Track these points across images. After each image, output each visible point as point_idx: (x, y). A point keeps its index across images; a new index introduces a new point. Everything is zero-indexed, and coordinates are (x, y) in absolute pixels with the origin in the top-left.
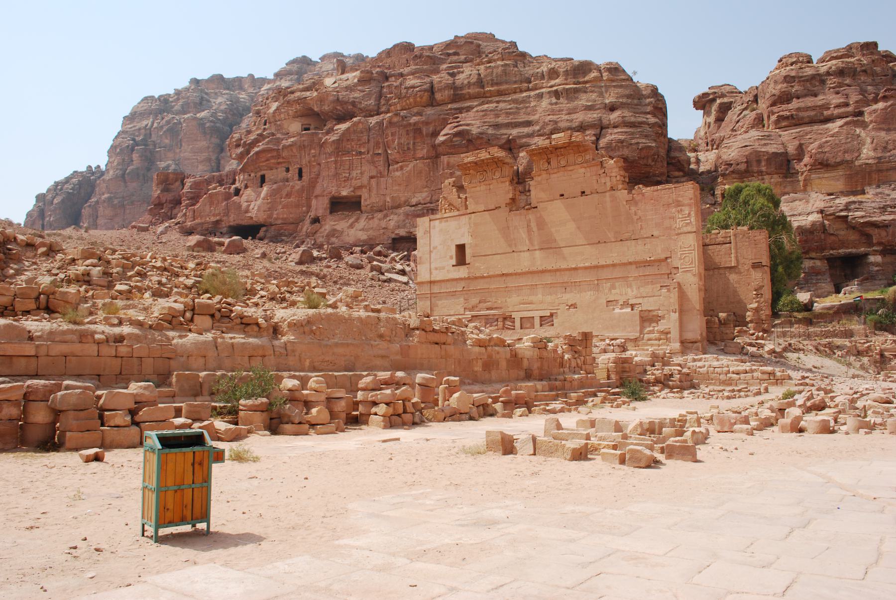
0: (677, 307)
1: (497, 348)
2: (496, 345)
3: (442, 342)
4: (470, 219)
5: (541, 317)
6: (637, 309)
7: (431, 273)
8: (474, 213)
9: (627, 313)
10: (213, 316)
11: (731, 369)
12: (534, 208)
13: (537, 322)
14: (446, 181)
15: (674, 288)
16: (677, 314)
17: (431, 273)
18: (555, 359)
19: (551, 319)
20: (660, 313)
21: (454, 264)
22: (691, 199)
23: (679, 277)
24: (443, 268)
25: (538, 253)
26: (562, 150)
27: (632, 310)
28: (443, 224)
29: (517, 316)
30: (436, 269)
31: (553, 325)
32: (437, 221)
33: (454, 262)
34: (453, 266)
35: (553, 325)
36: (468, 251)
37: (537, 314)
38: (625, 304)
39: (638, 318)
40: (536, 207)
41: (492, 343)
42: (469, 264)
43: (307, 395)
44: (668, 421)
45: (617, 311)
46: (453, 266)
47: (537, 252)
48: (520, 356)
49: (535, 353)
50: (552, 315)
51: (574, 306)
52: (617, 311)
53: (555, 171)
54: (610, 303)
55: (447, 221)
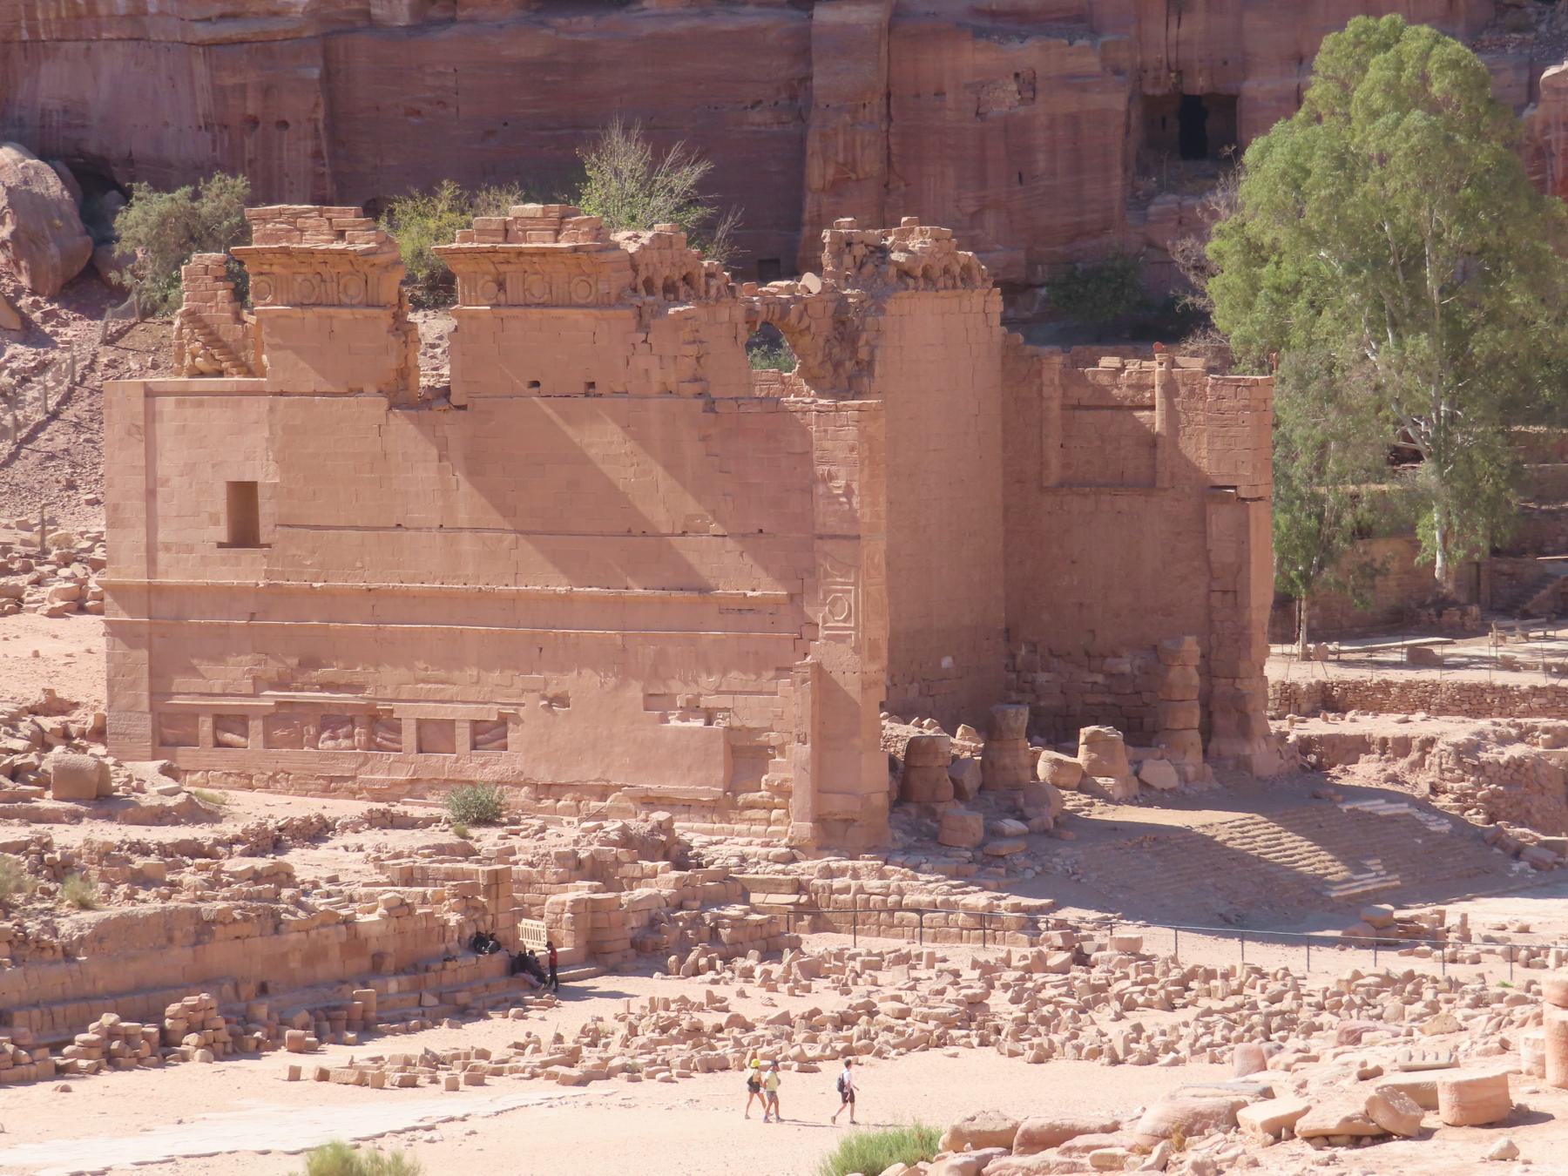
0: (807, 728)
1: (323, 930)
2: (323, 925)
3: (245, 934)
4: (272, 410)
5: (475, 723)
6: (720, 725)
7: (152, 561)
8: (282, 394)
9: (694, 731)
10: (10, 942)
11: (908, 899)
12: (459, 408)
13: (463, 736)
14: (195, 257)
15: (804, 681)
16: (808, 745)
17: (152, 561)
18: (428, 931)
19: (500, 730)
20: (773, 737)
21: (225, 540)
22: (852, 449)
23: (819, 650)
24: (190, 549)
25: (467, 543)
26: (535, 259)
27: (709, 723)
28: (189, 412)
29: (408, 714)
30: (167, 548)
31: (505, 748)
32: (173, 398)
33: (222, 533)
34: (221, 545)
35: (505, 748)
36: (267, 509)
37: (462, 713)
38: (691, 709)
39: (720, 745)
40: (464, 407)
41: (317, 922)
42: (269, 546)
43: (126, 1028)
44: (1201, 970)
45: (674, 723)
46: (221, 545)
47: (466, 535)
48: (362, 936)
49: (391, 927)
50: (503, 721)
51: (561, 700)
52: (674, 723)
53: (516, 311)
54: (654, 699)
55: (200, 405)
